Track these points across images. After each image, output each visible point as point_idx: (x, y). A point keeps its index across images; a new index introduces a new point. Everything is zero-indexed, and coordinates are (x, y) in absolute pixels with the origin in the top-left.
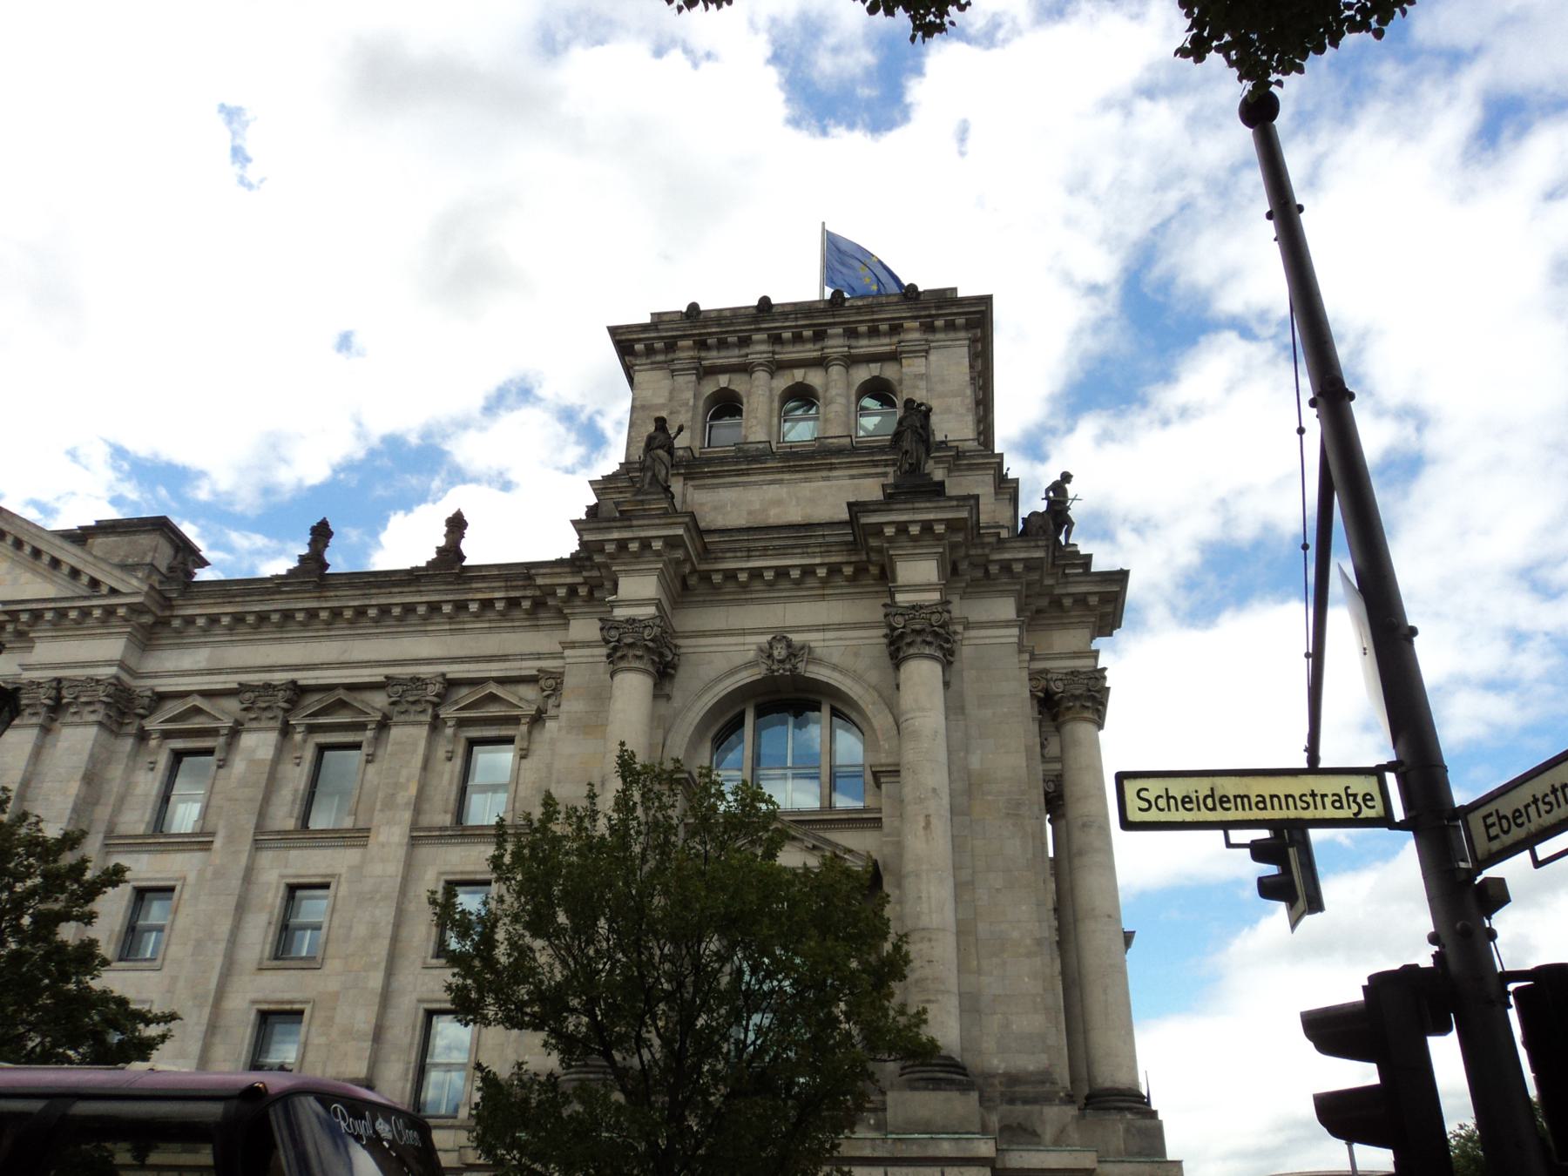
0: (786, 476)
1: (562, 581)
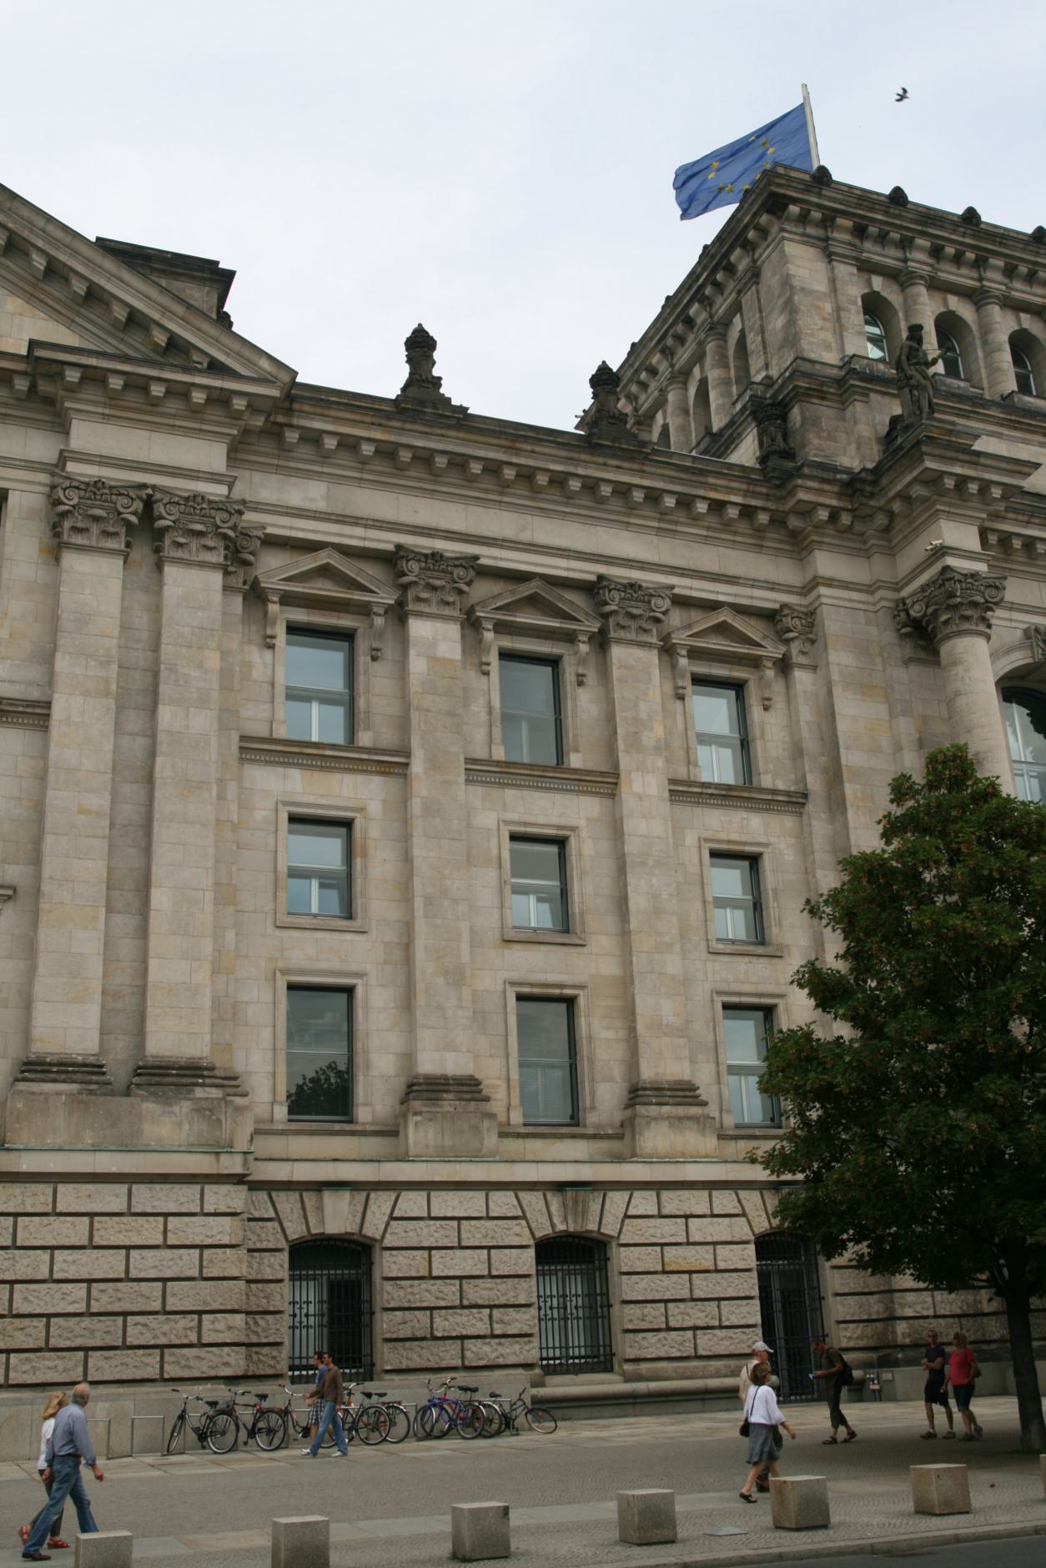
0: (1006, 431)
1: (827, 501)
